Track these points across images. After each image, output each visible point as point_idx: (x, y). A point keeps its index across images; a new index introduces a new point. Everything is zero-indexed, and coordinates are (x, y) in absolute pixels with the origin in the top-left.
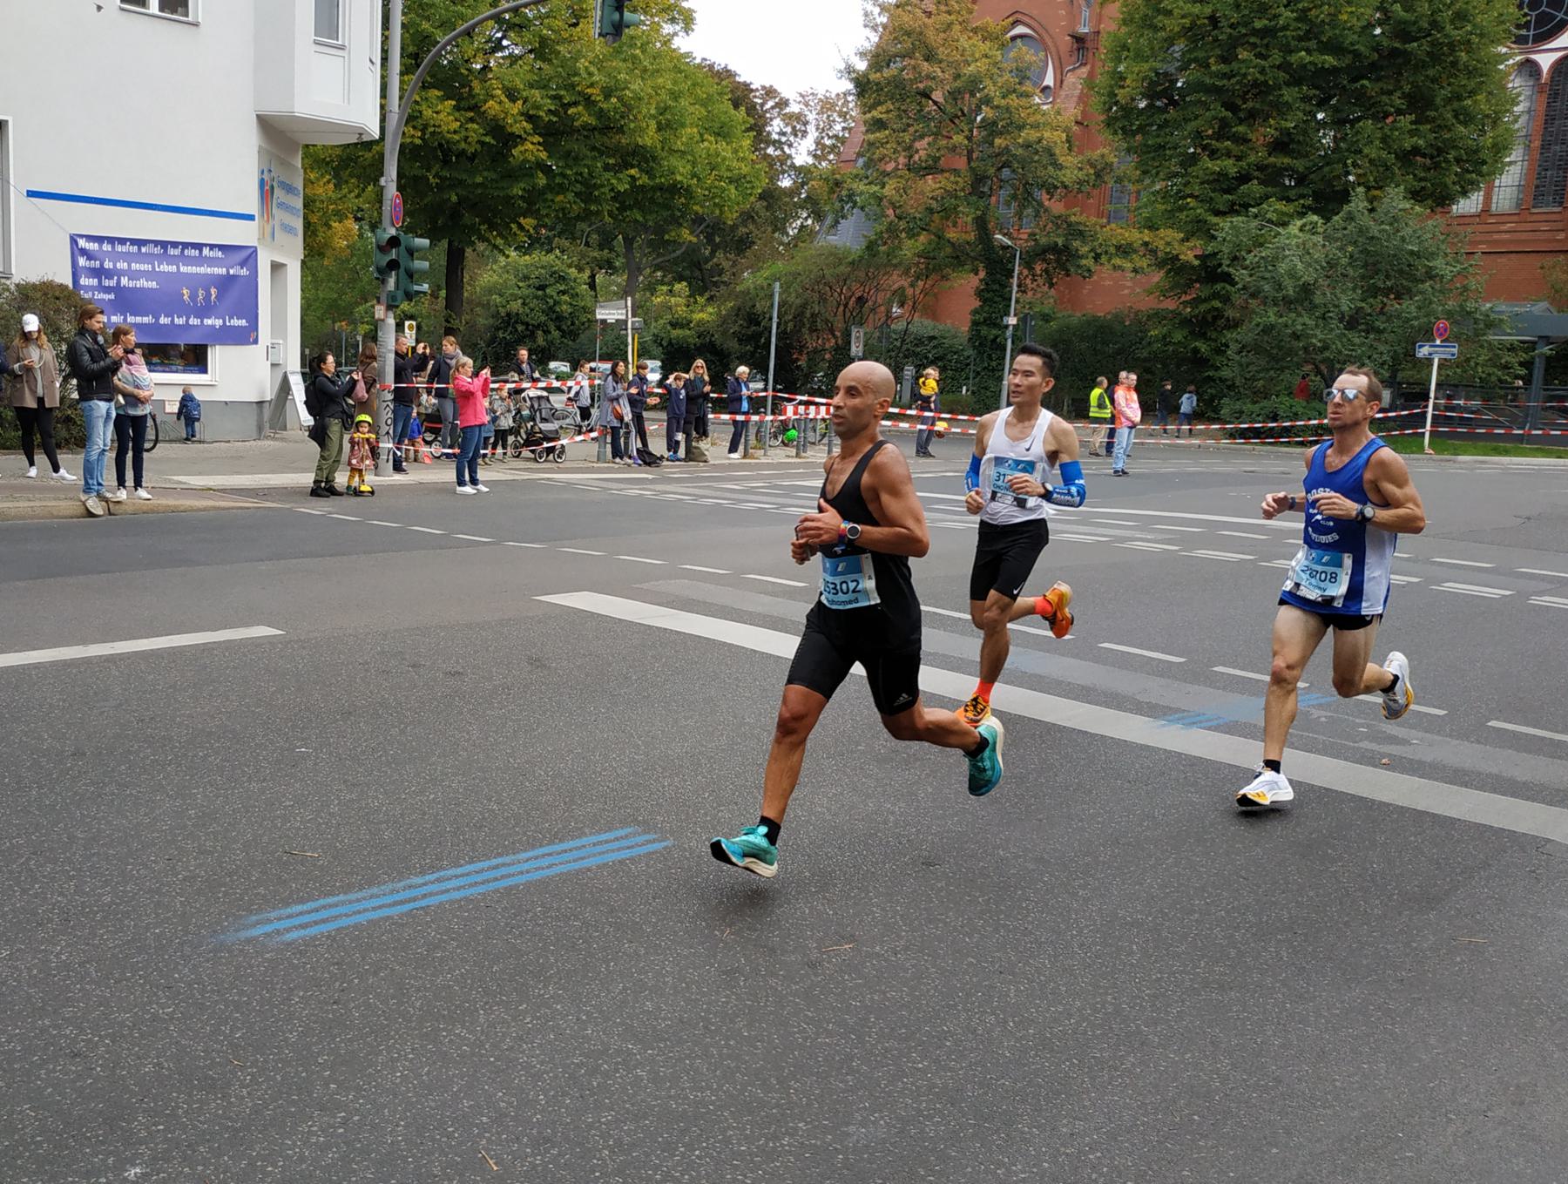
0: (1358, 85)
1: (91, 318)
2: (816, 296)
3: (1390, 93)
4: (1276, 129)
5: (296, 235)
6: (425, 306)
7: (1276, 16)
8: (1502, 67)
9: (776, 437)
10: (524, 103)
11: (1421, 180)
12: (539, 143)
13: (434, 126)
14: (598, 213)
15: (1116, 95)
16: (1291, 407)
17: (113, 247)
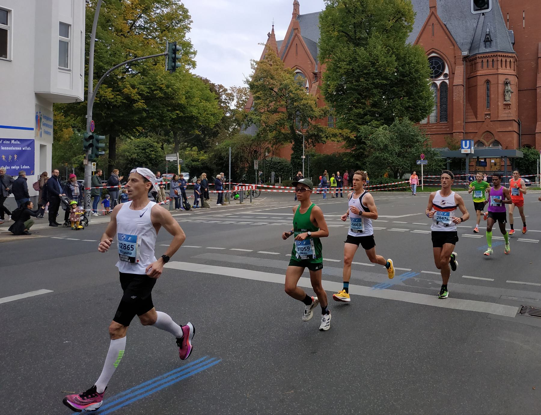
0: (393, 89)
2: (241, 150)
3: (401, 91)
4: (372, 101)
5: (50, 135)
7: (369, 70)
8: (428, 84)
9: (232, 197)
10: (138, 89)
11: (412, 115)
12: (143, 103)
13: (104, 97)
14: (165, 125)
15: (328, 91)
16: (386, 180)
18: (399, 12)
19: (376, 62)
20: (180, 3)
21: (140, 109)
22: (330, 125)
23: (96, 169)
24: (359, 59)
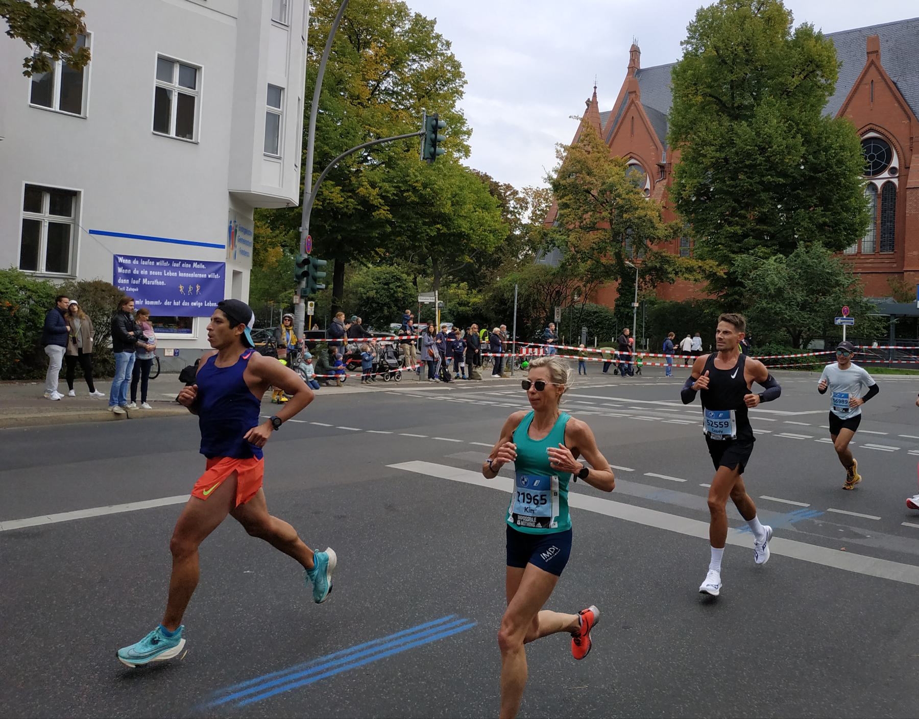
0: (796, 192)
1: (126, 304)
2: (535, 290)
3: (811, 196)
4: (759, 212)
5: (248, 256)
6: (319, 294)
8: (860, 186)
10: (380, 189)
12: (388, 210)
13: (330, 199)
14: (420, 247)
15: (682, 194)
17: (140, 262)
18: (811, 62)
19: (767, 146)
20: (449, 53)
21: (381, 221)
22: (682, 253)
23: (315, 311)
24: (737, 141)
